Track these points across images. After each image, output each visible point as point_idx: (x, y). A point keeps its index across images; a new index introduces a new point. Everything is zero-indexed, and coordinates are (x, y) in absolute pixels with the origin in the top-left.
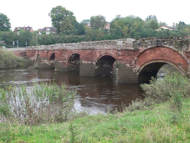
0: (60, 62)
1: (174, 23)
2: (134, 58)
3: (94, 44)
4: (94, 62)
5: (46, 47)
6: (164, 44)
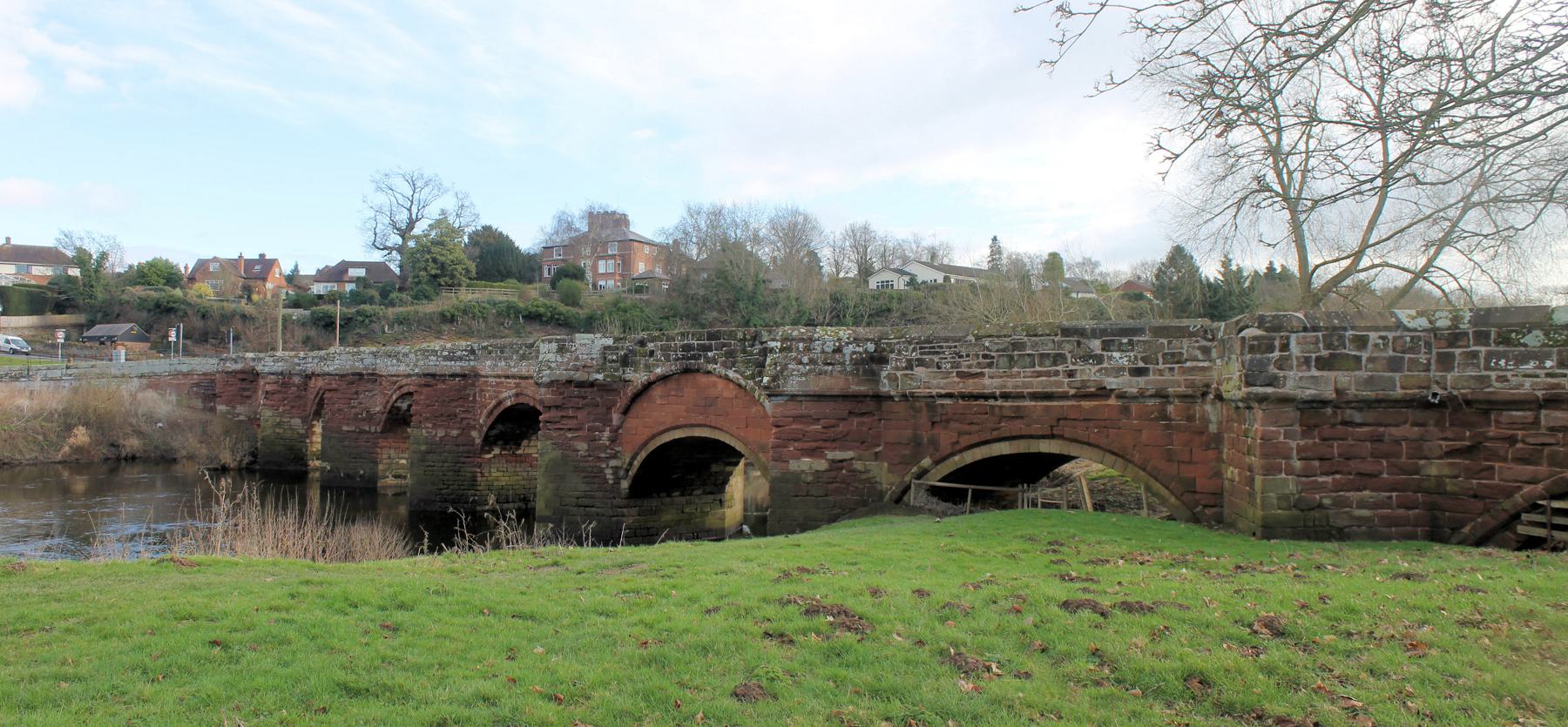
0: (345, 428)
2: (611, 420)
3: (472, 352)
4: (474, 434)
5: (296, 360)
6: (708, 361)
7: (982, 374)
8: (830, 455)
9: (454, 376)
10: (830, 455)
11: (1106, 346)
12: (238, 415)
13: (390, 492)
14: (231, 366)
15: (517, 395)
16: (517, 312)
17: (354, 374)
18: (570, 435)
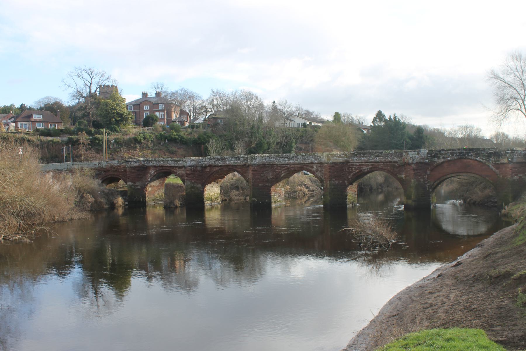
0: (260, 185)
1: (274, 102)
3: (346, 155)
4: (346, 182)
5: (199, 160)
6: (469, 156)
8: (519, 175)
10: (519, 175)
12: (137, 186)
13: (274, 208)
14: (134, 164)
15: (371, 168)
16: (165, 138)
17: (262, 164)
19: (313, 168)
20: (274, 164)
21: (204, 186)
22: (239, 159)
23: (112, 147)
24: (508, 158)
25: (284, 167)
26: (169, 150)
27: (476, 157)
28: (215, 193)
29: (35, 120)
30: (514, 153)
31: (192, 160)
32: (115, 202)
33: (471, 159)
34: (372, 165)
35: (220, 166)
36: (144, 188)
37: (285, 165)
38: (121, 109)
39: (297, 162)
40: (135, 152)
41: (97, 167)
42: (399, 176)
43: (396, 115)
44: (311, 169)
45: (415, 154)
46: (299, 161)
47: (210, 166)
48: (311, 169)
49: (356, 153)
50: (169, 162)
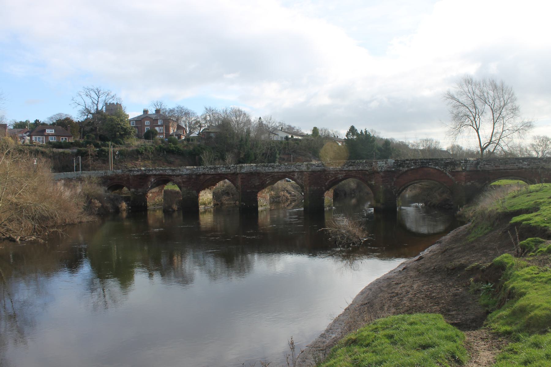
0: (248, 191)
1: (260, 118)
4: (323, 188)
5: (194, 169)
7: (500, 166)
9: (319, 171)
10: (472, 182)
11: (523, 161)
12: (139, 192)
13: (260, 211)
14: (136, 173)
15: (345, 176)
16: (164, 149)
18: (387, 184)
19: (295, 176)
20: (260, 172)
21: (198, 192)
22: (229, 168)
23: (117, 158)
24: (462, 167)
25: (269, 175)
26: (167, 160)
27: (435, 166)
28: (208, 198)
29: (48, 134)
30: (467, 162)
31: (187, 169)
32: (120, 206)
33: (431, 168)
34: (346, 173)
35: (212, 174)
36: (145, 194)
37: (269, 174)
38: (125, 124)
39: (281, 171)
40: (137, 162)
41: (103, 175)
42: (369, 182)
43: (366, 130)
44: (292, 177)
45: (384, 164)
46: (282, 169)
47: (204, 174)
48: (292, 177)
49: (332, 162)
50: (167, 171)
